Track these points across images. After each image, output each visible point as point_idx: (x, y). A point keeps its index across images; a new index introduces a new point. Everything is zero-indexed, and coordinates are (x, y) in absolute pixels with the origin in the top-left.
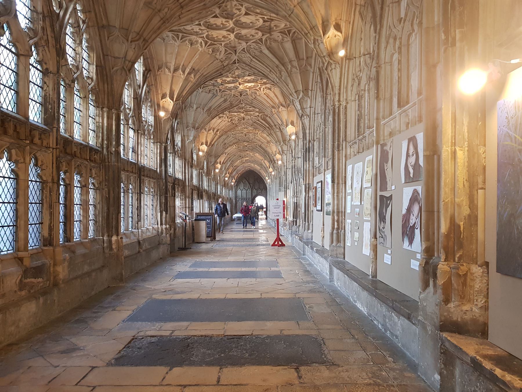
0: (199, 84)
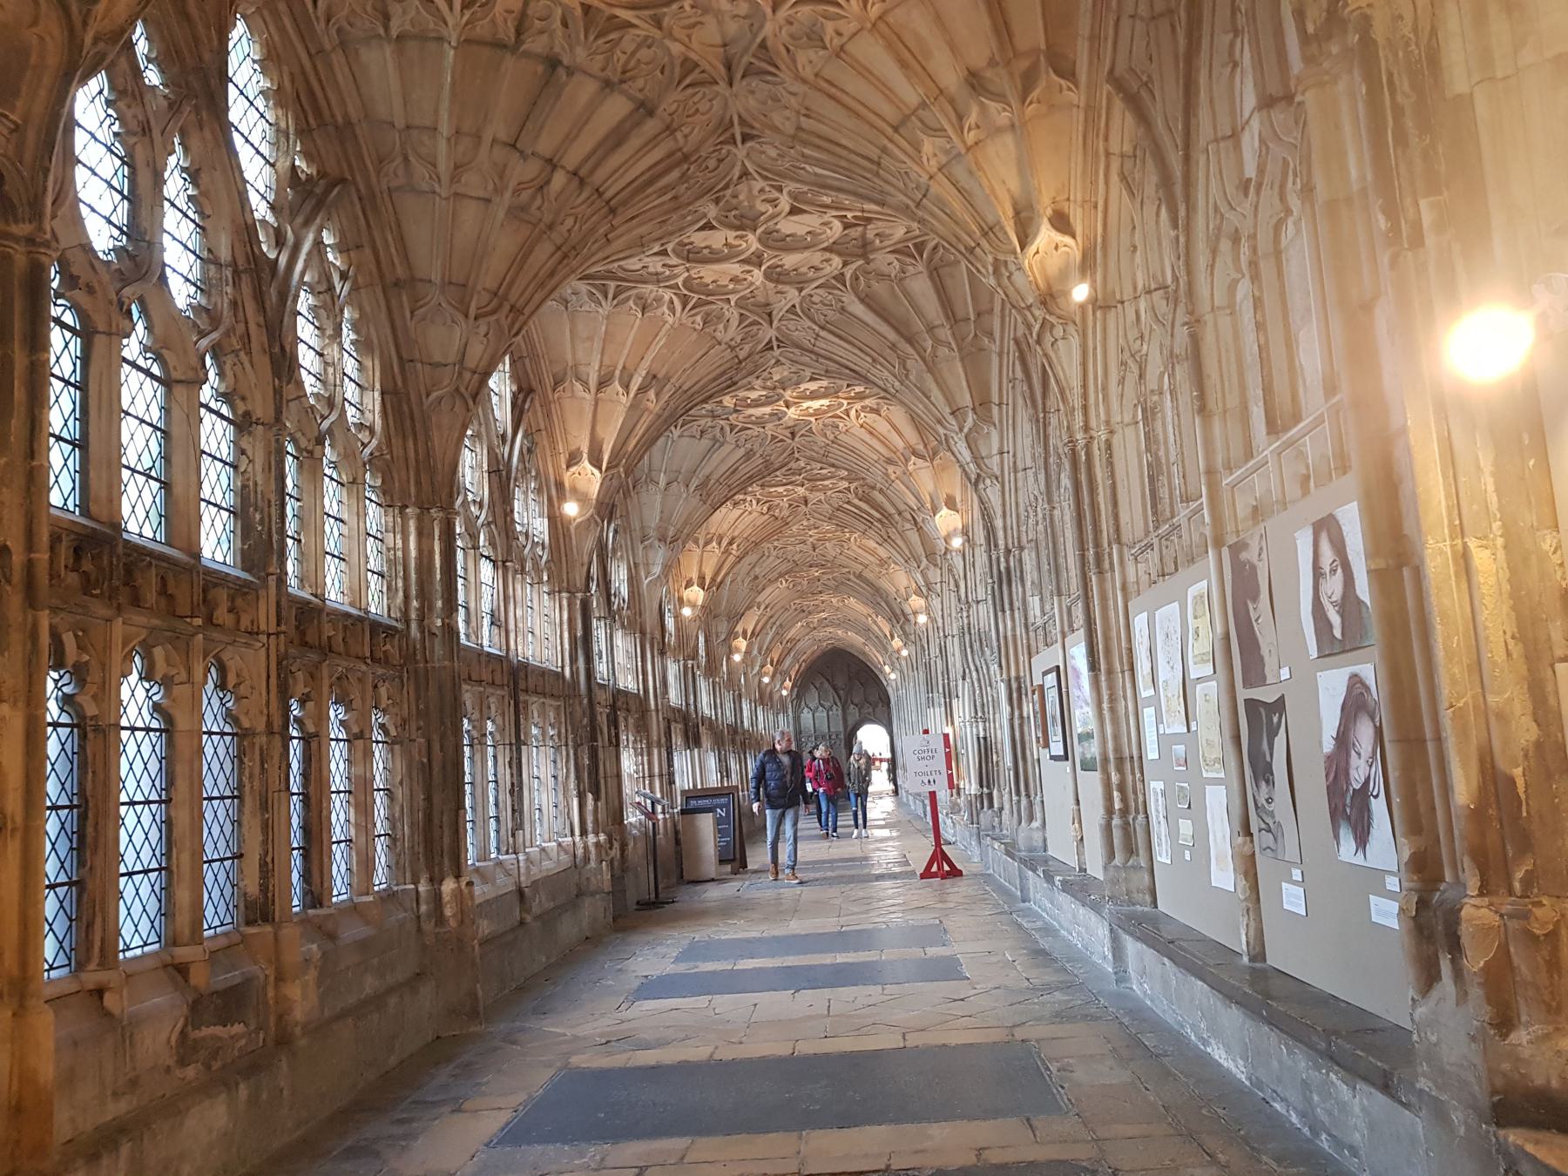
0: (671, 415)
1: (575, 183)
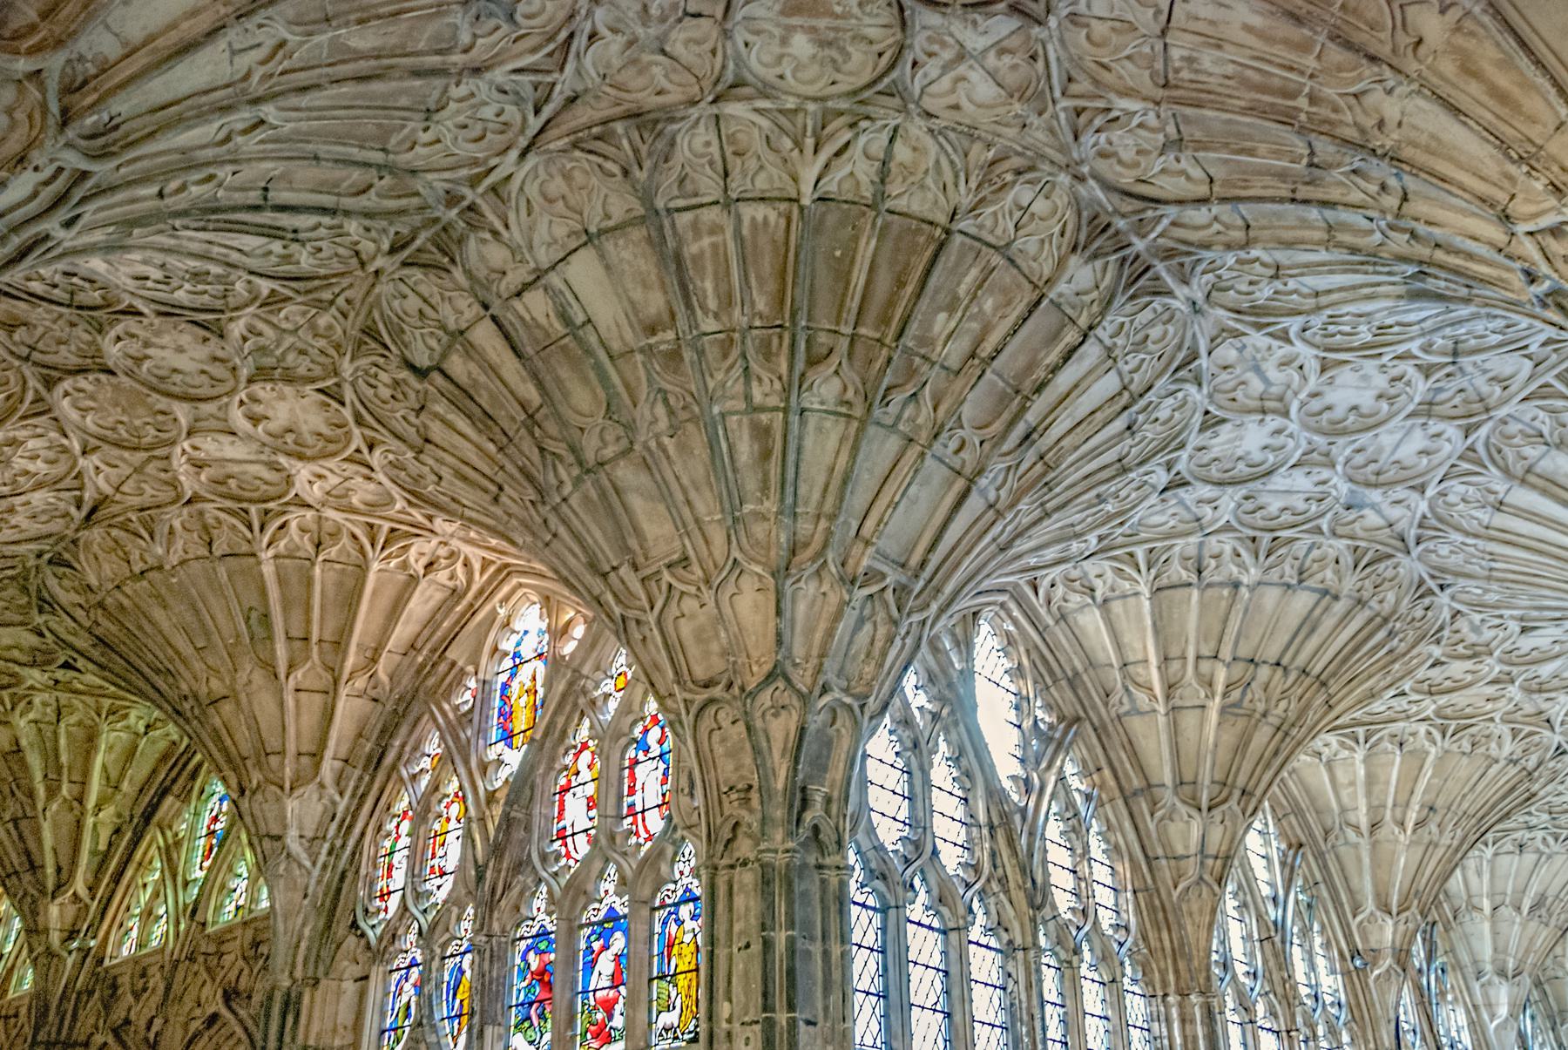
1: (1280, 671)
